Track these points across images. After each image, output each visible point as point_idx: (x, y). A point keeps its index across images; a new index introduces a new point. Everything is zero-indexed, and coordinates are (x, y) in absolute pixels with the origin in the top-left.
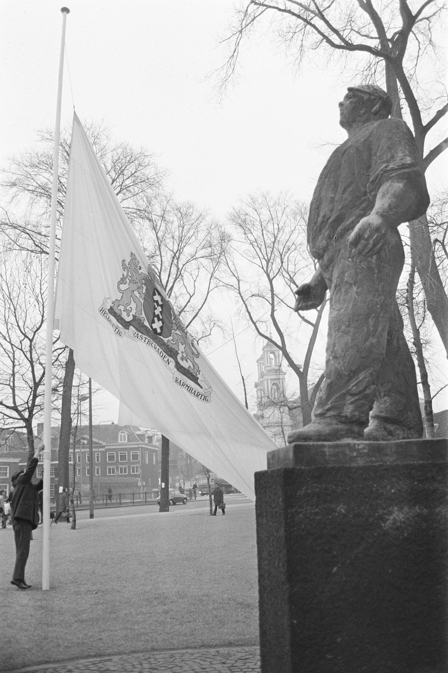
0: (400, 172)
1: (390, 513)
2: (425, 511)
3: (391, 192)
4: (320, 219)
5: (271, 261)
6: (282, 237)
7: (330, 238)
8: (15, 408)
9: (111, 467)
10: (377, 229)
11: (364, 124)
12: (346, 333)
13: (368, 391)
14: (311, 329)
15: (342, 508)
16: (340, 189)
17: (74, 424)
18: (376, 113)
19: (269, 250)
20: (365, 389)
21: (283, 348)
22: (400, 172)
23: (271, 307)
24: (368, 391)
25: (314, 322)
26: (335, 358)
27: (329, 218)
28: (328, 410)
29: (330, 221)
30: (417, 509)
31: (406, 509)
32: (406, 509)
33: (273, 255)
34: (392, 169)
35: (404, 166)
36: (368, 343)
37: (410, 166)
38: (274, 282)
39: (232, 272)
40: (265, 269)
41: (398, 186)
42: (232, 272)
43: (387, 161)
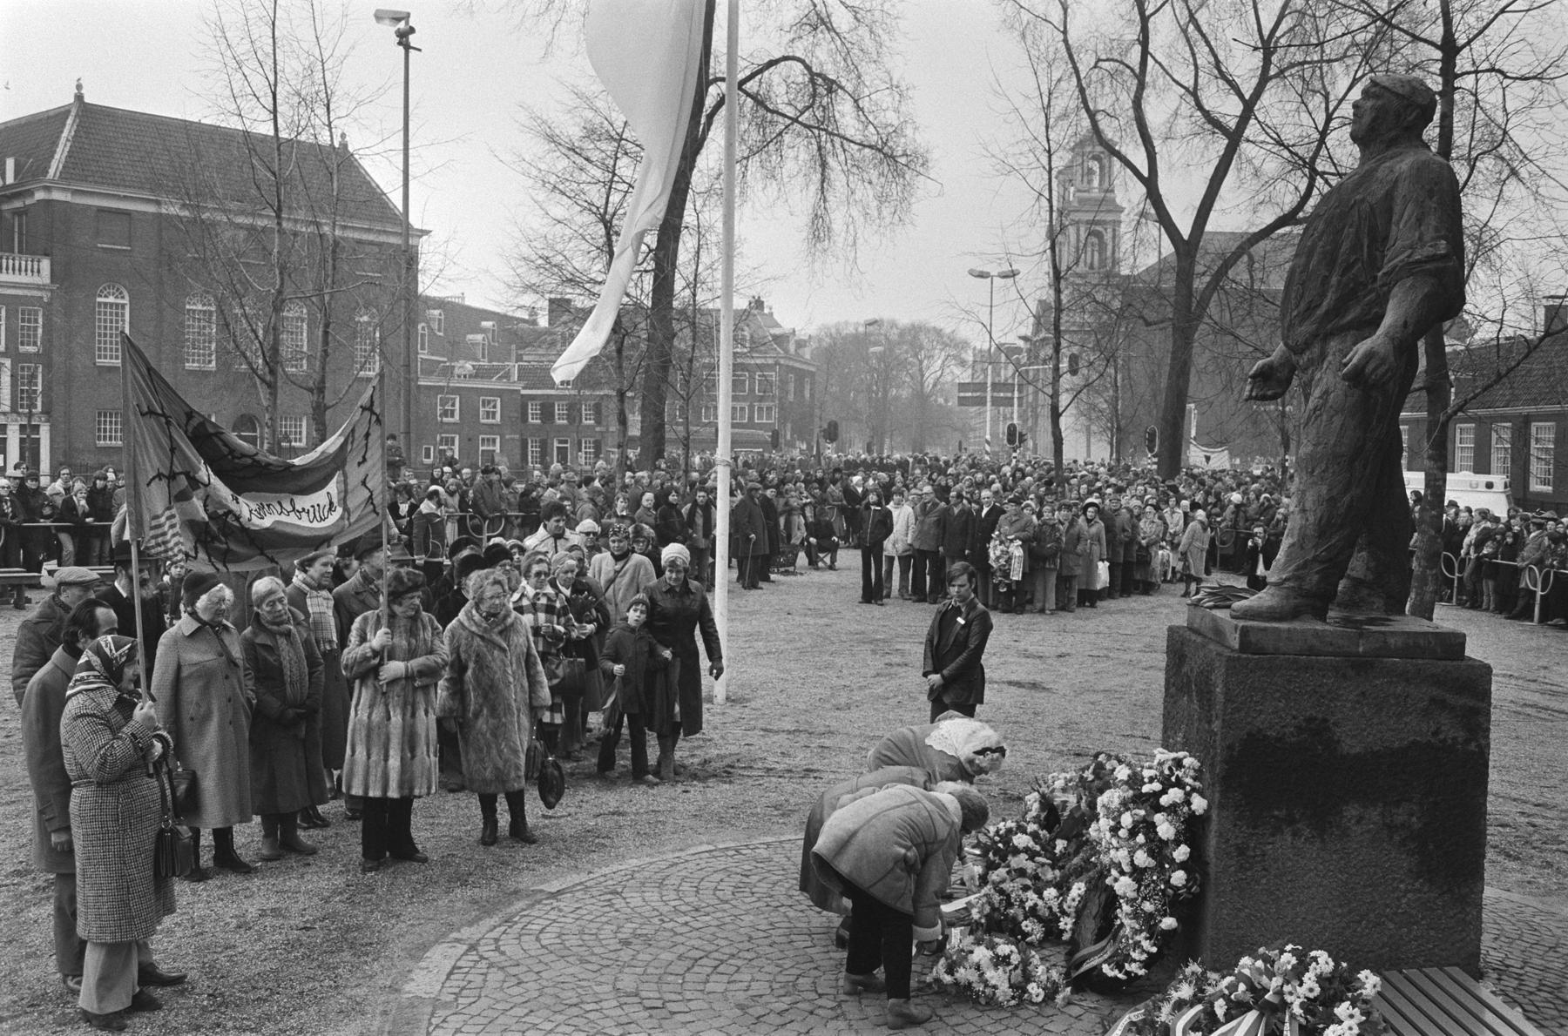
4: (1303, 306)
7: (1315, 336)
10: (1383, 361)
11: (1388, 147)
14: (1222, 143)
18: (1407, 129)
21: (1150, 183)
23: (1133, 84)
26: (1303, 511)
27: (1318, 306)
28: (1286, 580)
29: (1320, 312)
34: (1418, 262)
37: (1443, 257)
39: (1068, 48)
42: (1068, 48)
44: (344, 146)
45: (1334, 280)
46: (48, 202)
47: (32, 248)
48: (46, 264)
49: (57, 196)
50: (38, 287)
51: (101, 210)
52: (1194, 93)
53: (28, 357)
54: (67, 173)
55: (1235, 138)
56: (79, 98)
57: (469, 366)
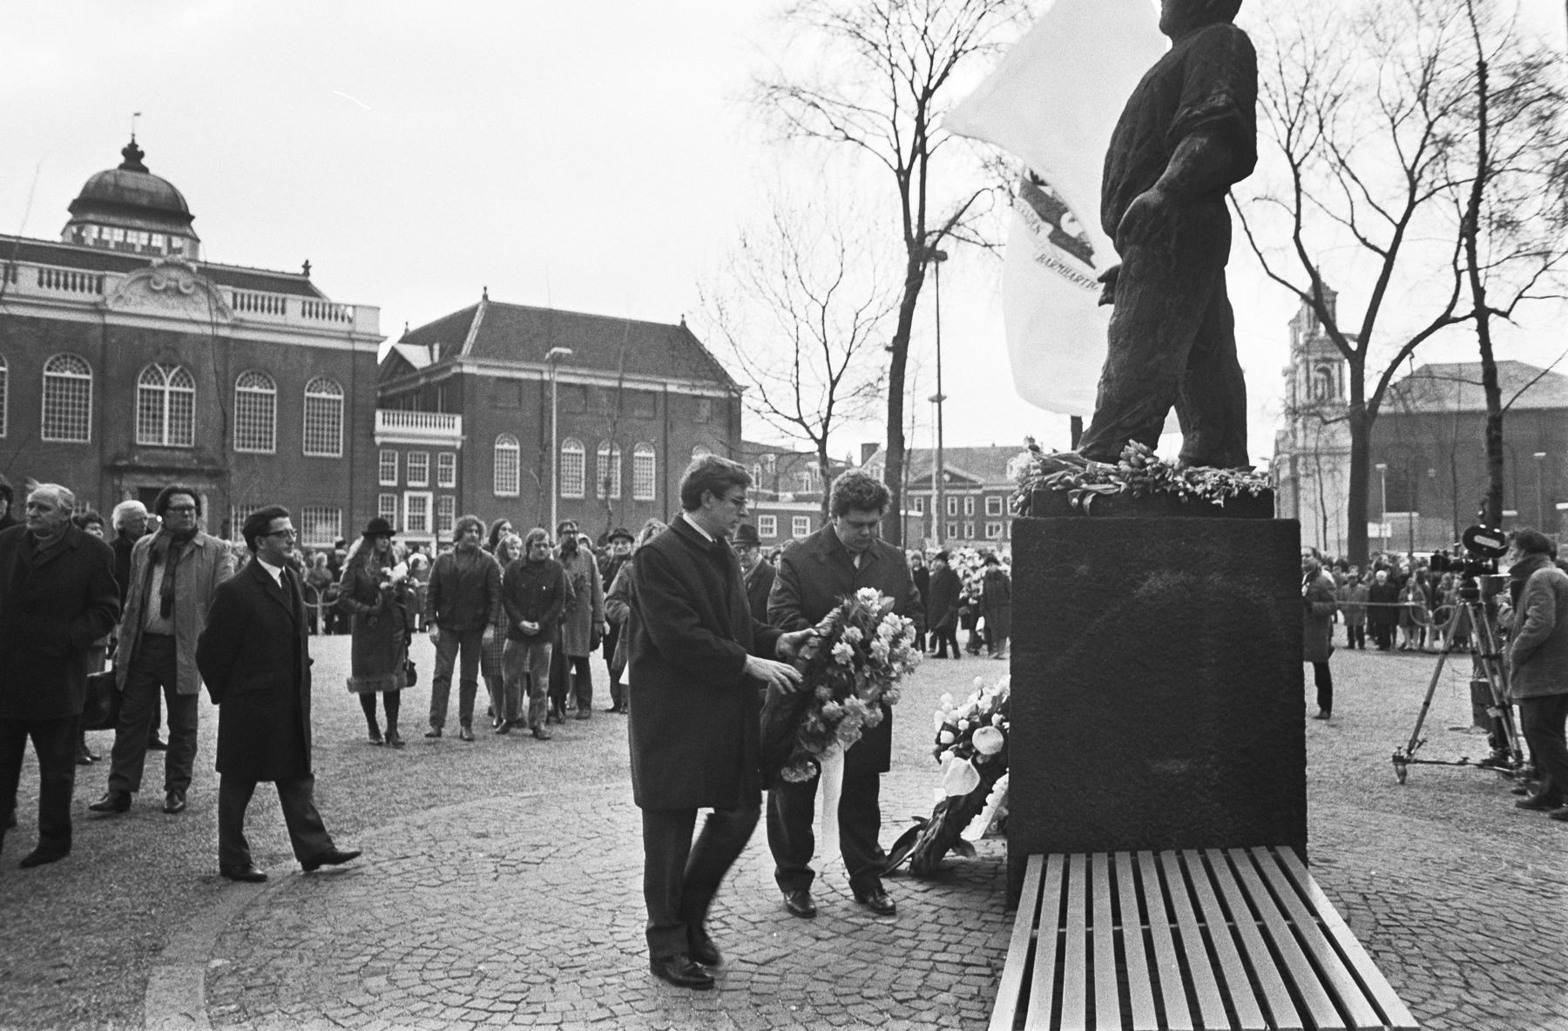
0: (1205, 121)
1: (1145, 579)
2: (1192, 578)
3: (1188, 152)
5: (1298, 124)
6: (1321, 76)
8: (800, 420)
9: (994, 524)
10: (1157, 210)
12: (1124, 347)
13: (1147, 425)
15: (1083, 569)
16: (1135, 143)
17: (907, 447)
19: (1294, 102)
20: (1143, 422)
22: (1205, 121)
24: (1147, 425)
25: (1386, 249)
30: (1181, 576)
31: (1166, 575)
32: (1166, 575)
33: (1302, 114)
34: (1197, 116)
35: (1214, 111)
36: (1151, 363)
38: (1301, 170)
40: (1284, 143)
41: (1198, 143)
43: (1192, 105)
44: (683, 323)
45: (1130, 154)
46: (462, 375)
47: (450, 409)
48: (458, 420)
49: (466, 369)
50: (454, 439)
51: (499, 379)
52: (1352, 225)
53: (447, 491)
54: (474, 353)
55: (1390, 257)
56: (485, 297)
57: (790, 495)
